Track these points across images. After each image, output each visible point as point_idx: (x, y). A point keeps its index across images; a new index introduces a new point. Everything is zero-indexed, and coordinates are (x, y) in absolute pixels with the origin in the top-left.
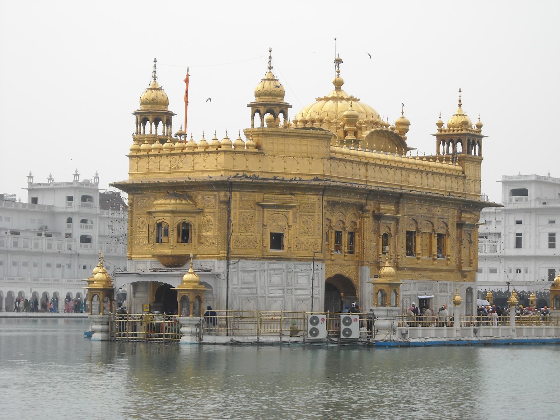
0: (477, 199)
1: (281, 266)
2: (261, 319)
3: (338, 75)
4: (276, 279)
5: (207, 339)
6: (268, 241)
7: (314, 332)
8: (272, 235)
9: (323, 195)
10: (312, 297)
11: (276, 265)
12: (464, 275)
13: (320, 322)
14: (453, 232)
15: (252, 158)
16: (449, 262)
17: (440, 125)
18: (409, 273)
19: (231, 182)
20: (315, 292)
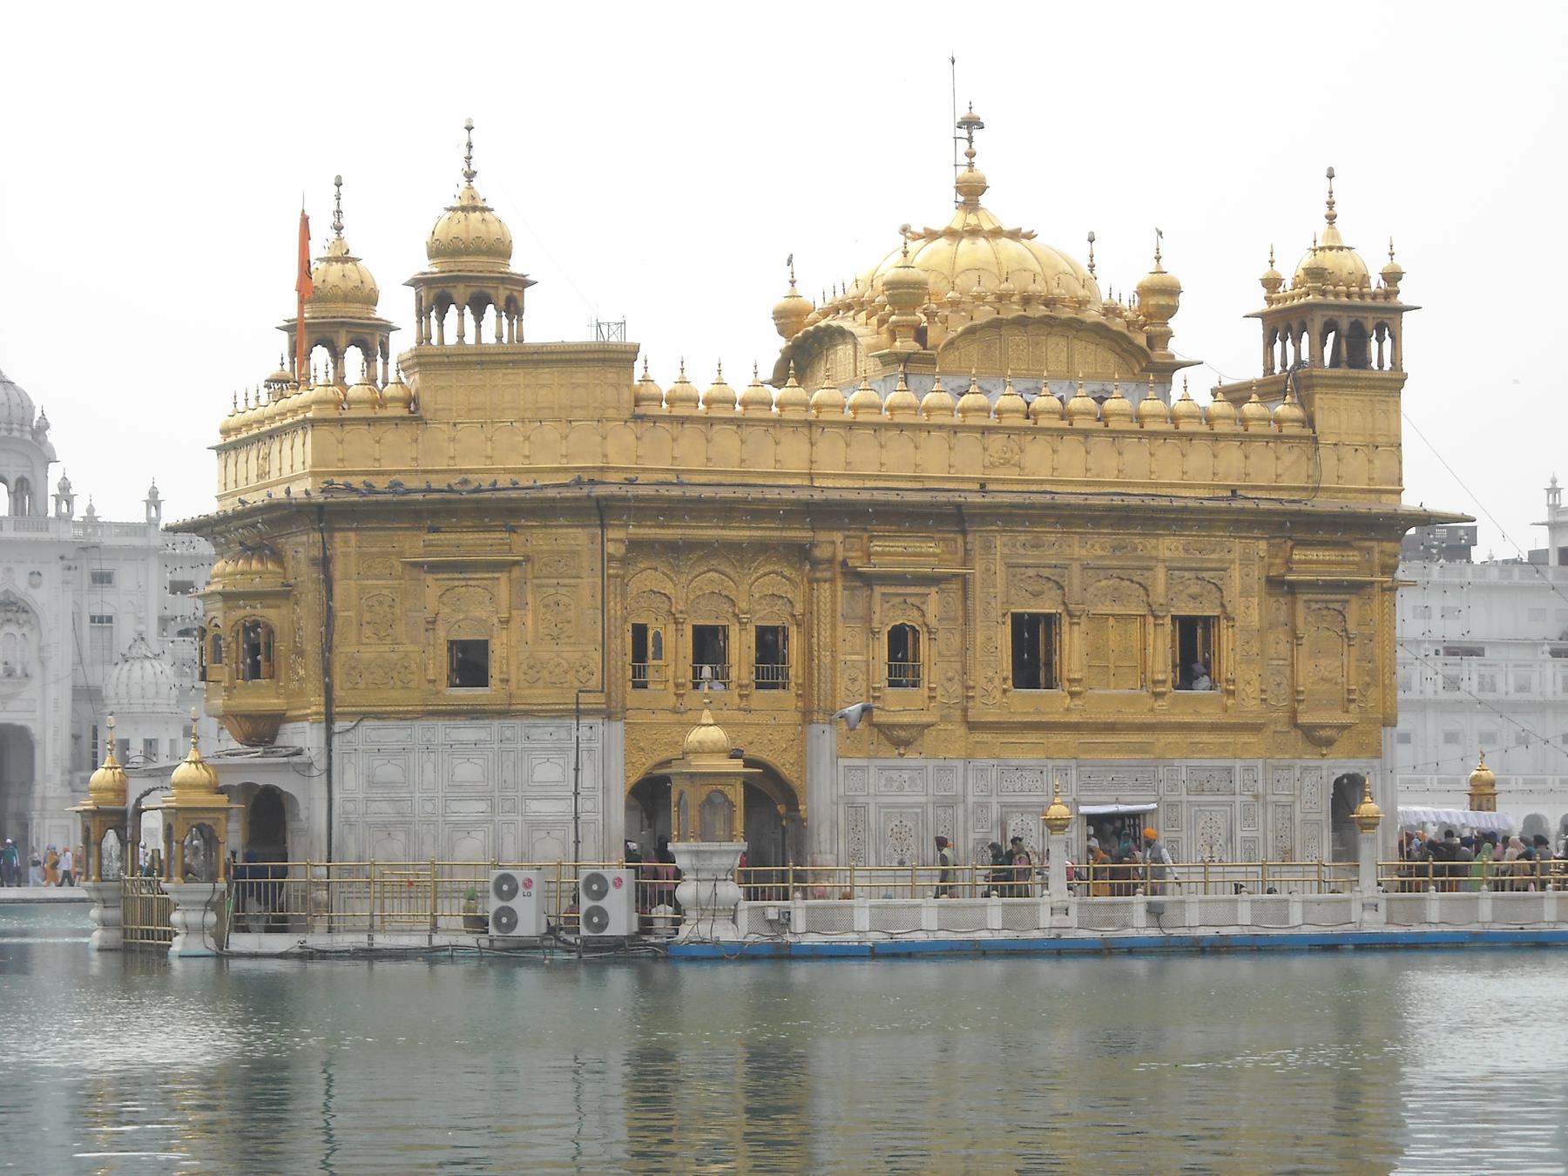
0: (1383, 505)
1: (483, 735)
2: (422, 886)
3: (971, 165)
4: (468, 771)
5: (240, 942)
6: (439, 663)
7: (508, 918)
8: (453, 645)
9: (603, 526)
10: (576, 818)
11: (467, 732)
12: (1317, 739)
13: (521, 889)
14: (1247, 607)
15: (390, 436)
16: (1230, 702)
17: (1272, 283)
18: (1032, 737)
19: (320, 508)
20: (585, 805)
